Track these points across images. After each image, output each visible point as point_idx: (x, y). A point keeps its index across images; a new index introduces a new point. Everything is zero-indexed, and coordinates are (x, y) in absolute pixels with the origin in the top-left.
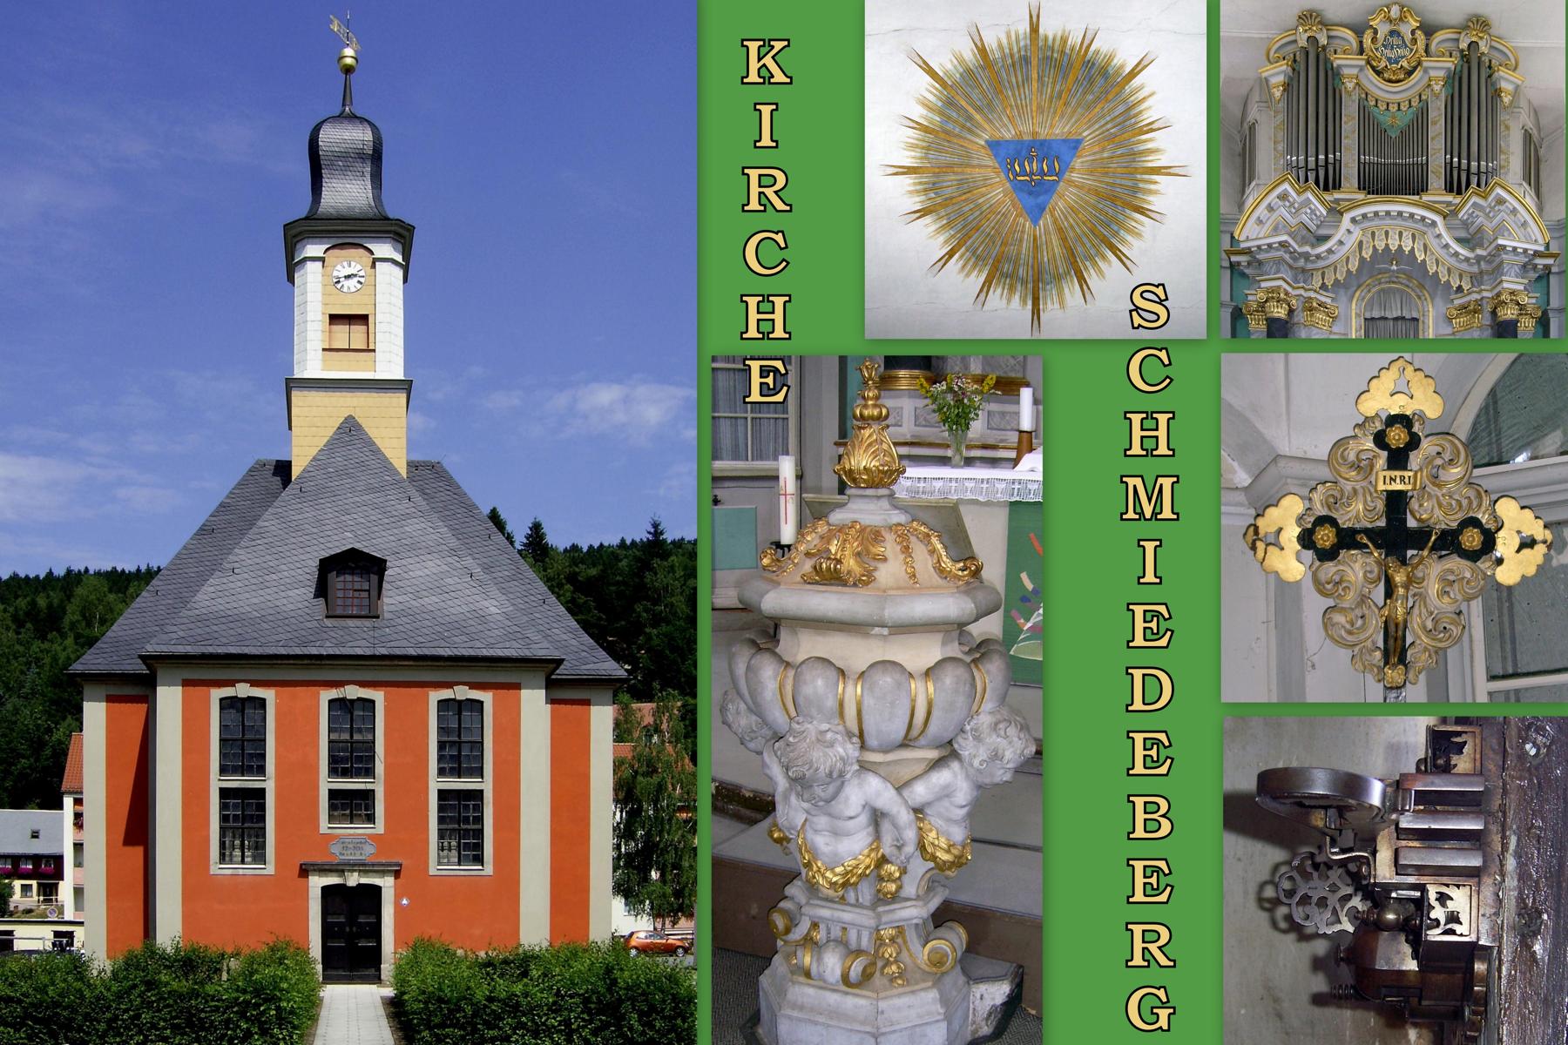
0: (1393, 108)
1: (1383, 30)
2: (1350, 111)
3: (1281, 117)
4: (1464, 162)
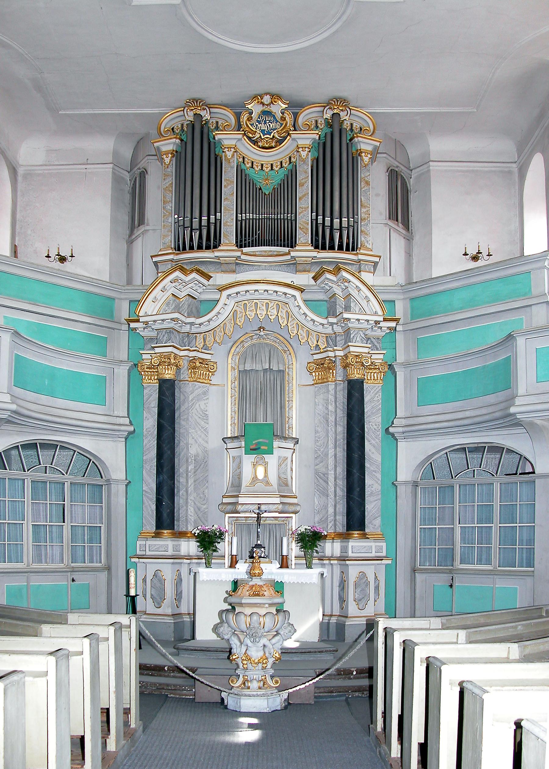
0: (267, 169)
1: (256, 108)
2: (229, 176)
3: (171, 180)
4: (328, 219)
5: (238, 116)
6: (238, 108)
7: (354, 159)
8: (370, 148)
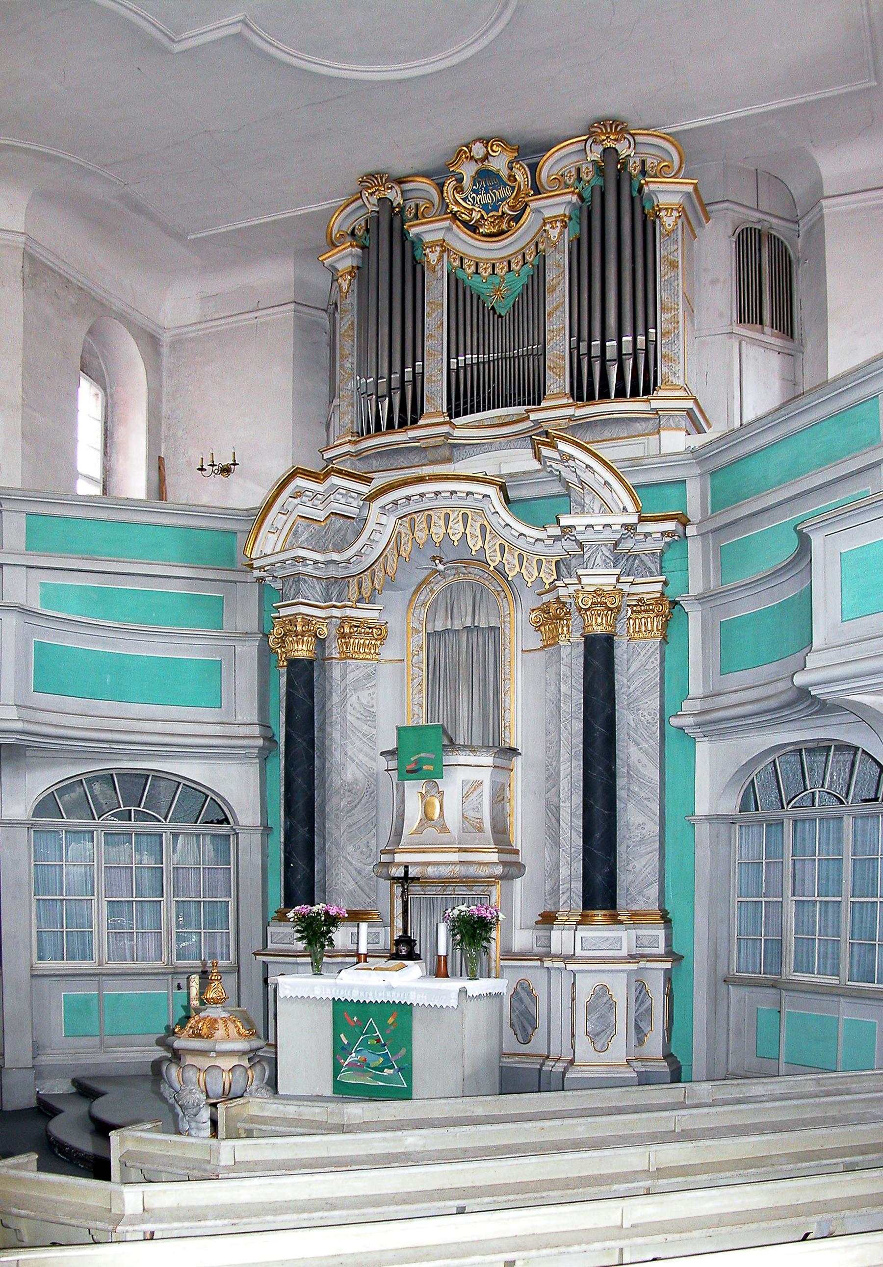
5: (441, 187)
6: (439, 175)
7: (646, 225)
8: (676, 200)
